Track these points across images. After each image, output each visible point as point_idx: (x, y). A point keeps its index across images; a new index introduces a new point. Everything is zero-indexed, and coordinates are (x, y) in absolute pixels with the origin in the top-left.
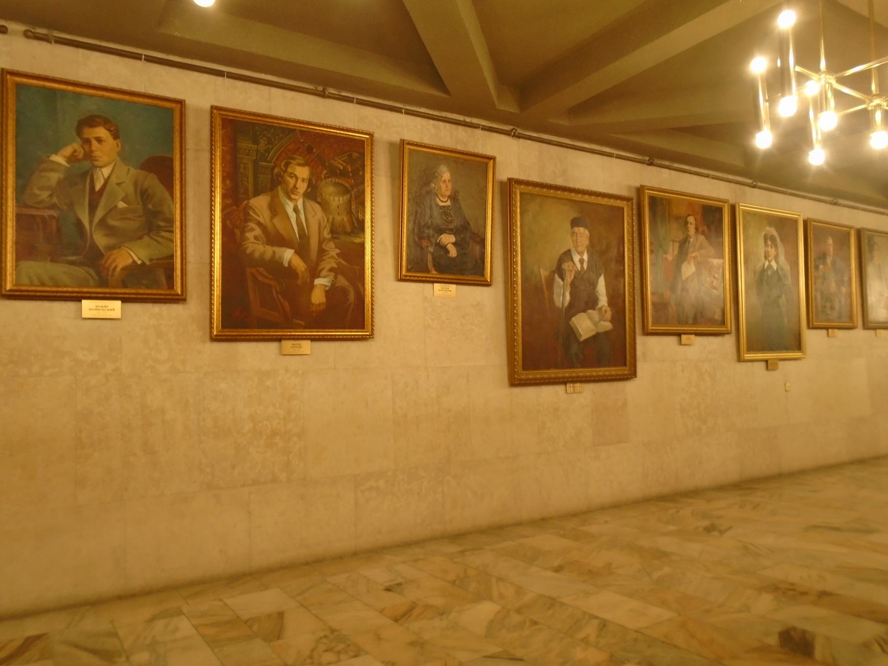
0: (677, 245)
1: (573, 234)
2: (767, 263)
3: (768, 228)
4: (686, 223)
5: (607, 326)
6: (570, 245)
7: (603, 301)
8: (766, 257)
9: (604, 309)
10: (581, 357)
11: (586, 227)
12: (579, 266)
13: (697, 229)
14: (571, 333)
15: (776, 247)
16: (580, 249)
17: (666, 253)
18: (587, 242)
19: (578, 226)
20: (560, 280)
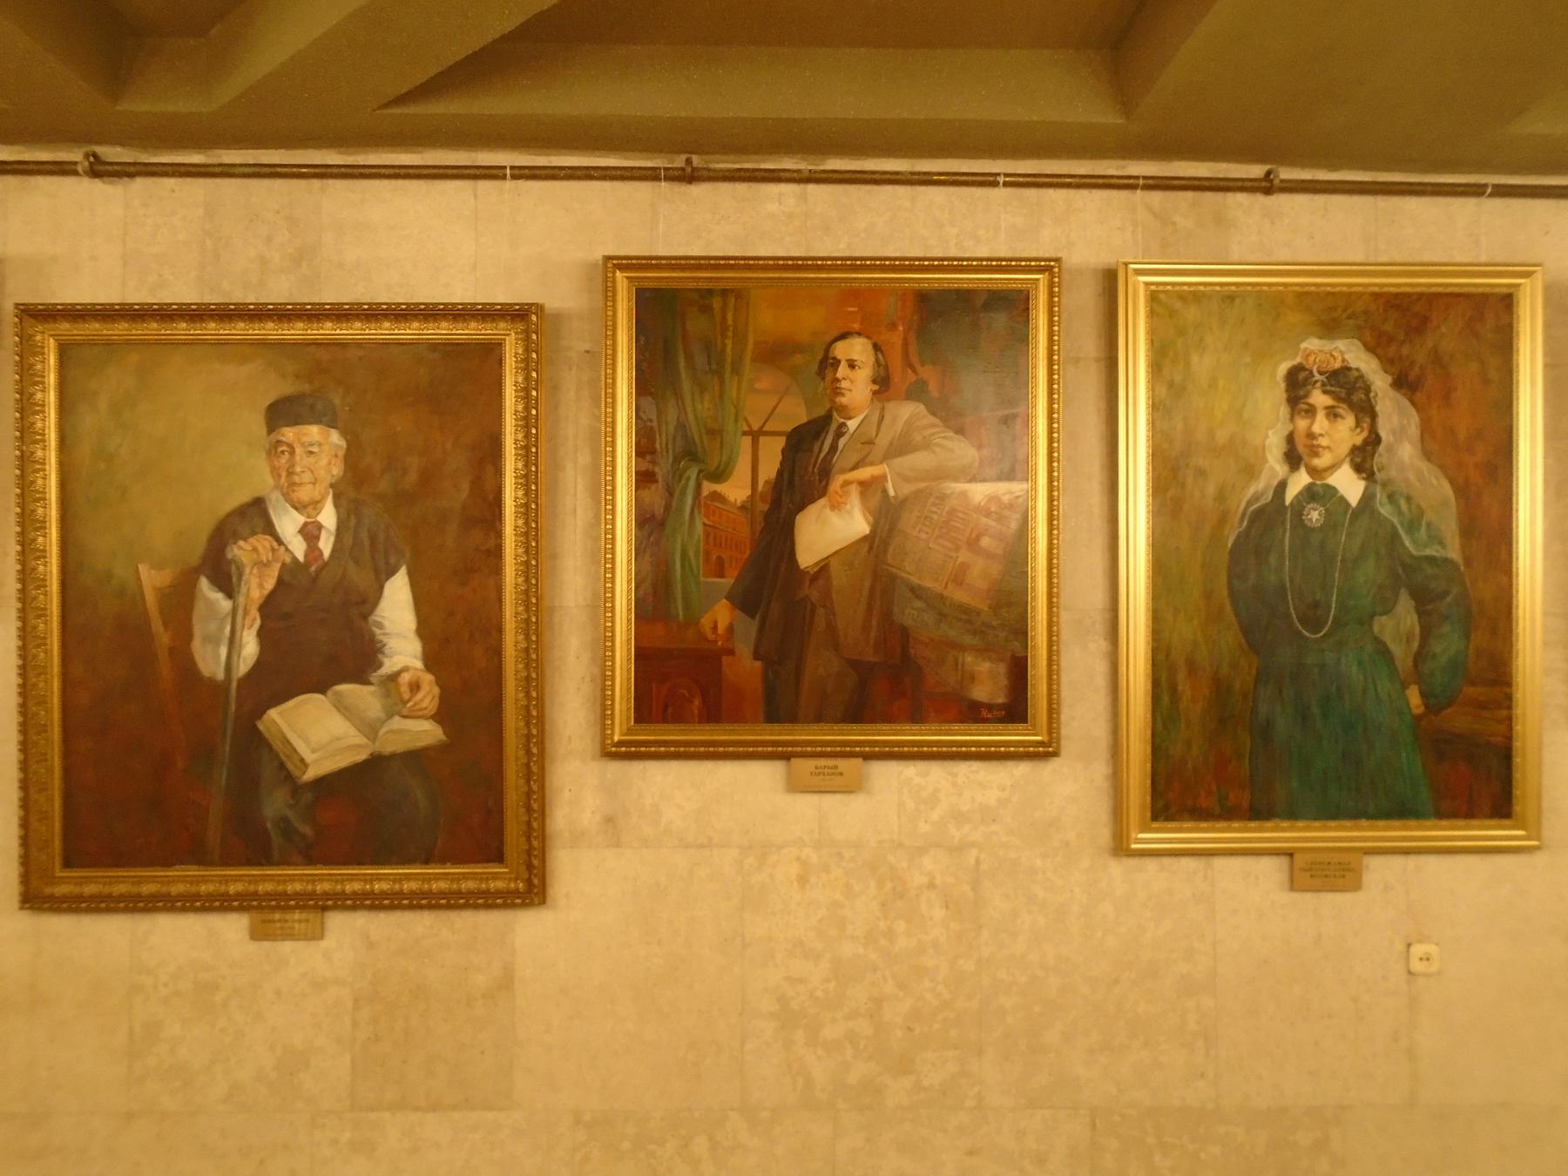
1: (274, 449)
2: (1301, 480)
3: (1313, 344)
4: (828, 363)
5: (424, 732)
6: (258, 478)
8: (1293, 459)
9: (405, 678)
10: (307, 830)
12: (298, 548)
14: (256, 755)
15: (1365, 410)
17: (719, 476)
18: (337, 470)
19: (296, 420)
20: (218, 597)
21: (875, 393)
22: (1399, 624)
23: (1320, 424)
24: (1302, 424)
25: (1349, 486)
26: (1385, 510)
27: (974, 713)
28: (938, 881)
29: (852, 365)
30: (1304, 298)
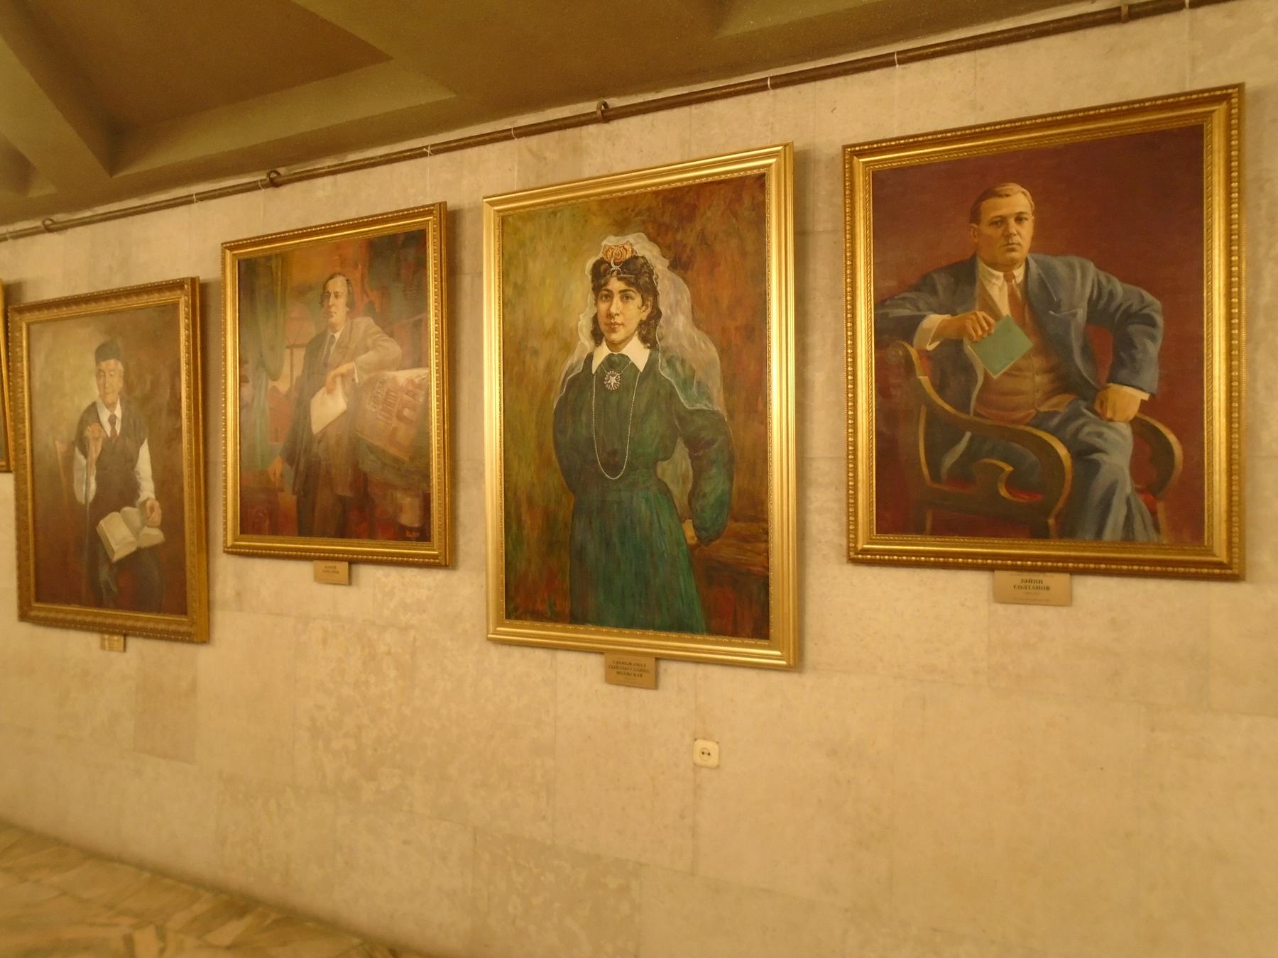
0: (300, 354)
2: (603, 352)
3: (611, 241)
4: (325, 295)
5: (154, 535)
7: (148, 490)
8: (597, 336)
9: (149, 503)
10: (115, 589)
11: (118, 358)
12: (108, 428)
13: (350, 304)
14: (96, 544)
16: (110, 399)
17: (275, 377)
18: (121, 385)
19: (106, 358)
21: (348, 313)
22: (676, 469)
23: (616, 305)
24: (603, 306)
25: (637, 354)
26: (665, 373)
27: (401, 534)
28: (393, 650)
29: (336, 296)
30: (604, 203)
